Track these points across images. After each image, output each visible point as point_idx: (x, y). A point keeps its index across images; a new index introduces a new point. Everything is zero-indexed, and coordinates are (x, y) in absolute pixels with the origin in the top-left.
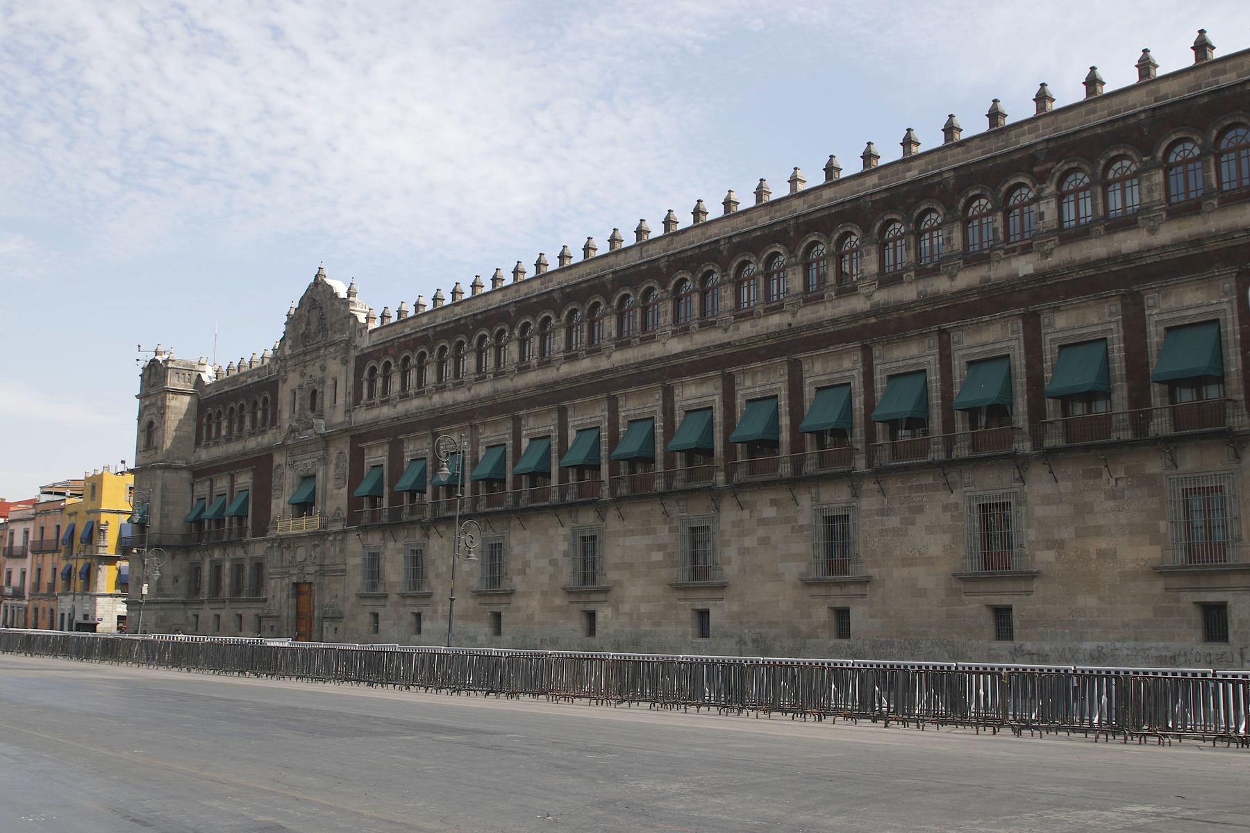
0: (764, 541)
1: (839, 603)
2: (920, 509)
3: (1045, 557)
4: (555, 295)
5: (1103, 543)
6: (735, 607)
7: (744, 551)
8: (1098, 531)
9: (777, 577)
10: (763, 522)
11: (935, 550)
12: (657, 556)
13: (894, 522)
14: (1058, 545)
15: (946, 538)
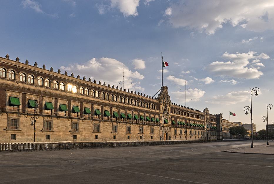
0: (106, 128)
1: (115, 135)
2: (123, 126)
3: (132, 132)
4: (52, 76)
5: (136, 131)
6: (102, 135)
7: (103, 128)
8: (135, 130)
9: (108, 132)
10: (106, 125)
11: (124, 130)
12: (90, 128)
13: (121, 127)
14: (133, 131)
15: (125, 129)
